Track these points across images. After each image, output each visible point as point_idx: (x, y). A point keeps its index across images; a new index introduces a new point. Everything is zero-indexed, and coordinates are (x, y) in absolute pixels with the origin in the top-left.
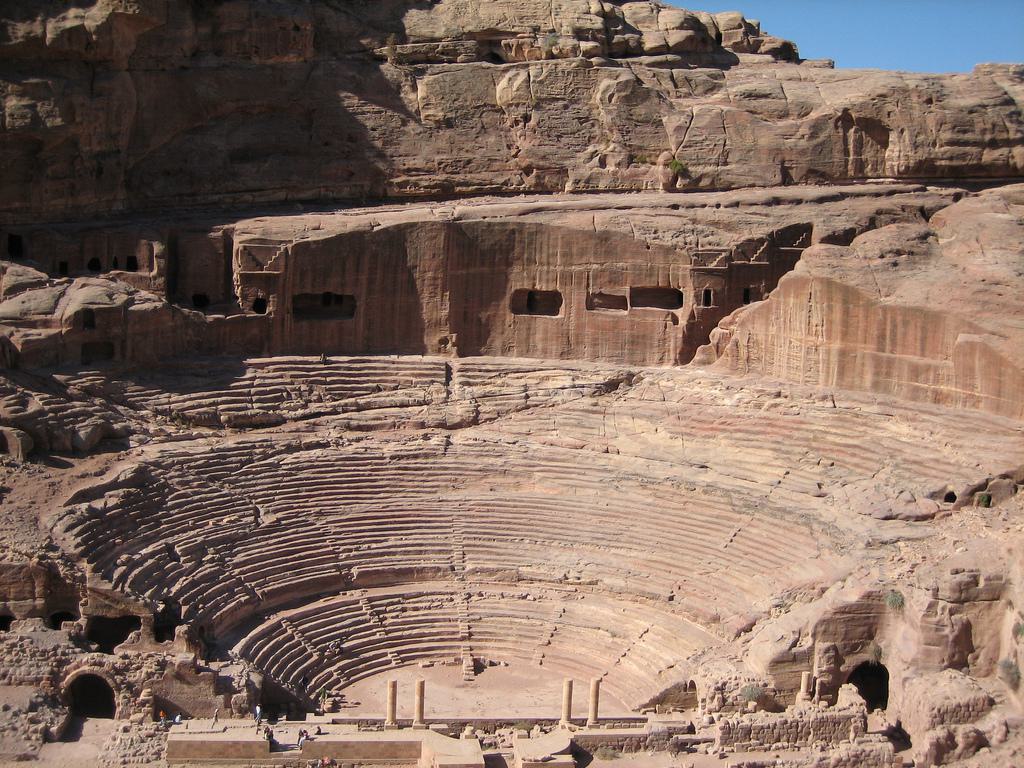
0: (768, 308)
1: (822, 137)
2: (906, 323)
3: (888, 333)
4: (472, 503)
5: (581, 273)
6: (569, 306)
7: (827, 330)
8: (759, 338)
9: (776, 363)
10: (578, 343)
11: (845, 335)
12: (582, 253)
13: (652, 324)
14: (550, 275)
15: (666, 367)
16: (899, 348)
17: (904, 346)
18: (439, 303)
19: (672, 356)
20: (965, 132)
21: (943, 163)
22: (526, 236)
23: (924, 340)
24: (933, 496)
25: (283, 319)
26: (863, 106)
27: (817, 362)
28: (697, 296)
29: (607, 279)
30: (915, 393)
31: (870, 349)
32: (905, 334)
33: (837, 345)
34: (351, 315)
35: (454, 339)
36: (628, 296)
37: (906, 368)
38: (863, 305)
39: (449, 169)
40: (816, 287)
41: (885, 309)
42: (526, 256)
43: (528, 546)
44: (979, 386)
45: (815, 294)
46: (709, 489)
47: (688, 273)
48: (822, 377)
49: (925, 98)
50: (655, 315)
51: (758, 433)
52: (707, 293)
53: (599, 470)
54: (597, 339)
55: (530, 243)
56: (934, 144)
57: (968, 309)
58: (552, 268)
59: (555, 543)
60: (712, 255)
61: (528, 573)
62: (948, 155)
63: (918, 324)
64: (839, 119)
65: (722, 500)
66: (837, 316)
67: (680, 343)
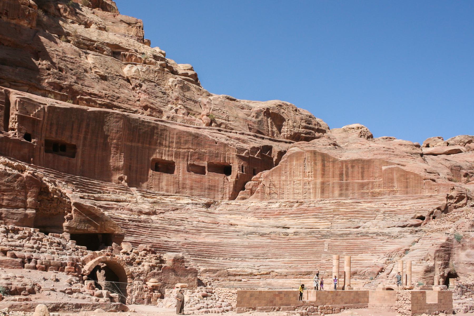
0: (280, 169)
1: (260, 119)
2: (353, 167)
3: (344, 172)
4: (181, 243)
5: (185, 153)
6: (179, 168)
7: (314, 174)
8: (276, 183)
9: (286, 192)
10: (183, 188)
11: (323, 175)
12: (186, 142)
13: (218, 180)
14: (170, 153)
16: (350, 178)
17: (352, 177)
18: (118, 158)
19: (228, 196)
20: (309, 124)
21: (303, 135)
22: (159, 130)
23: (362, 173)
24: (412, 218)
25: (40, 148)
26: (273, 108)
27: (309, 189)
28: (239, 167)
29: (197, 157)
30: (363, 195)
31: (337, 180)
32: (353, 172)
33: (319, 180)
34: (73, 156)
35: (126, 178)
36: (206, 166)
37: (356, 185)
38: (332, 161)
39: (110, 99)
40: (308, 155)
41: (342, 162)
42: (158, 141)
43: (223, 261)
44: (396, 186)
45: (308, 158)
46: (296, 233)
47: (235, 156)
48: (312, 196)
49: (295, 109)
50: (220, 177)
51: (301, 214)
52: (242, 166)
53: (233, 232)
54: (192, 186)
55: (161, 135)
56: (299, 128)
58: (170, 149)
59: (236, 259)
60: (242, 150)
61: (233, 271)
62: (305, 132)
63: (360, 167)
64: (265, 112)
65: (308, 236)
66: (319, 166)
67: (231, 189)
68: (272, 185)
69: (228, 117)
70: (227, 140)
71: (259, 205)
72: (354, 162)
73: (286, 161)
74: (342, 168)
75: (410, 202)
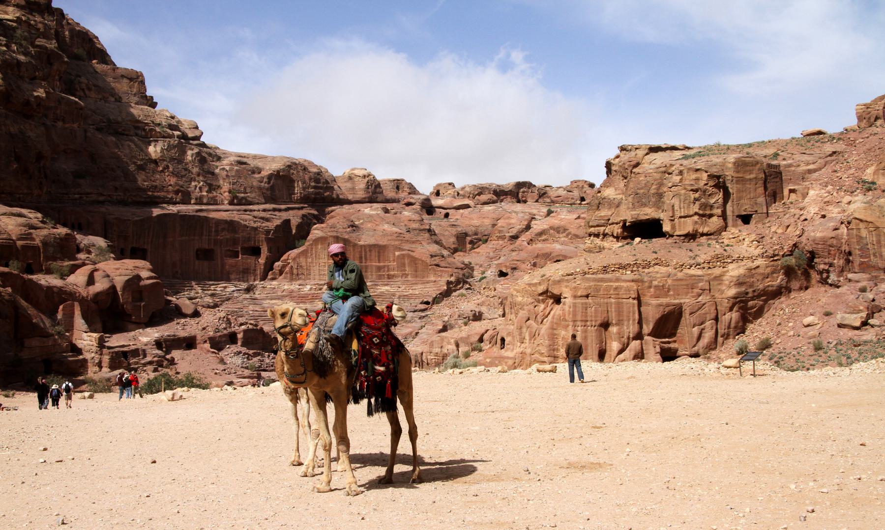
2: (370, 251)
9: (312, 274)
12: (223, 229)
15: (257, 282)
23: (379, 257)
30: (380, 277)
41: (361, 246)
50: (251, 260)
57: (397, 243)
68: (299, 266)
69: (245, 189)
70: (255, 222)
71: (292, 287)
72: (372, 247)
73: (312, 245)
74: (361, 252)
75: (420, 286)
